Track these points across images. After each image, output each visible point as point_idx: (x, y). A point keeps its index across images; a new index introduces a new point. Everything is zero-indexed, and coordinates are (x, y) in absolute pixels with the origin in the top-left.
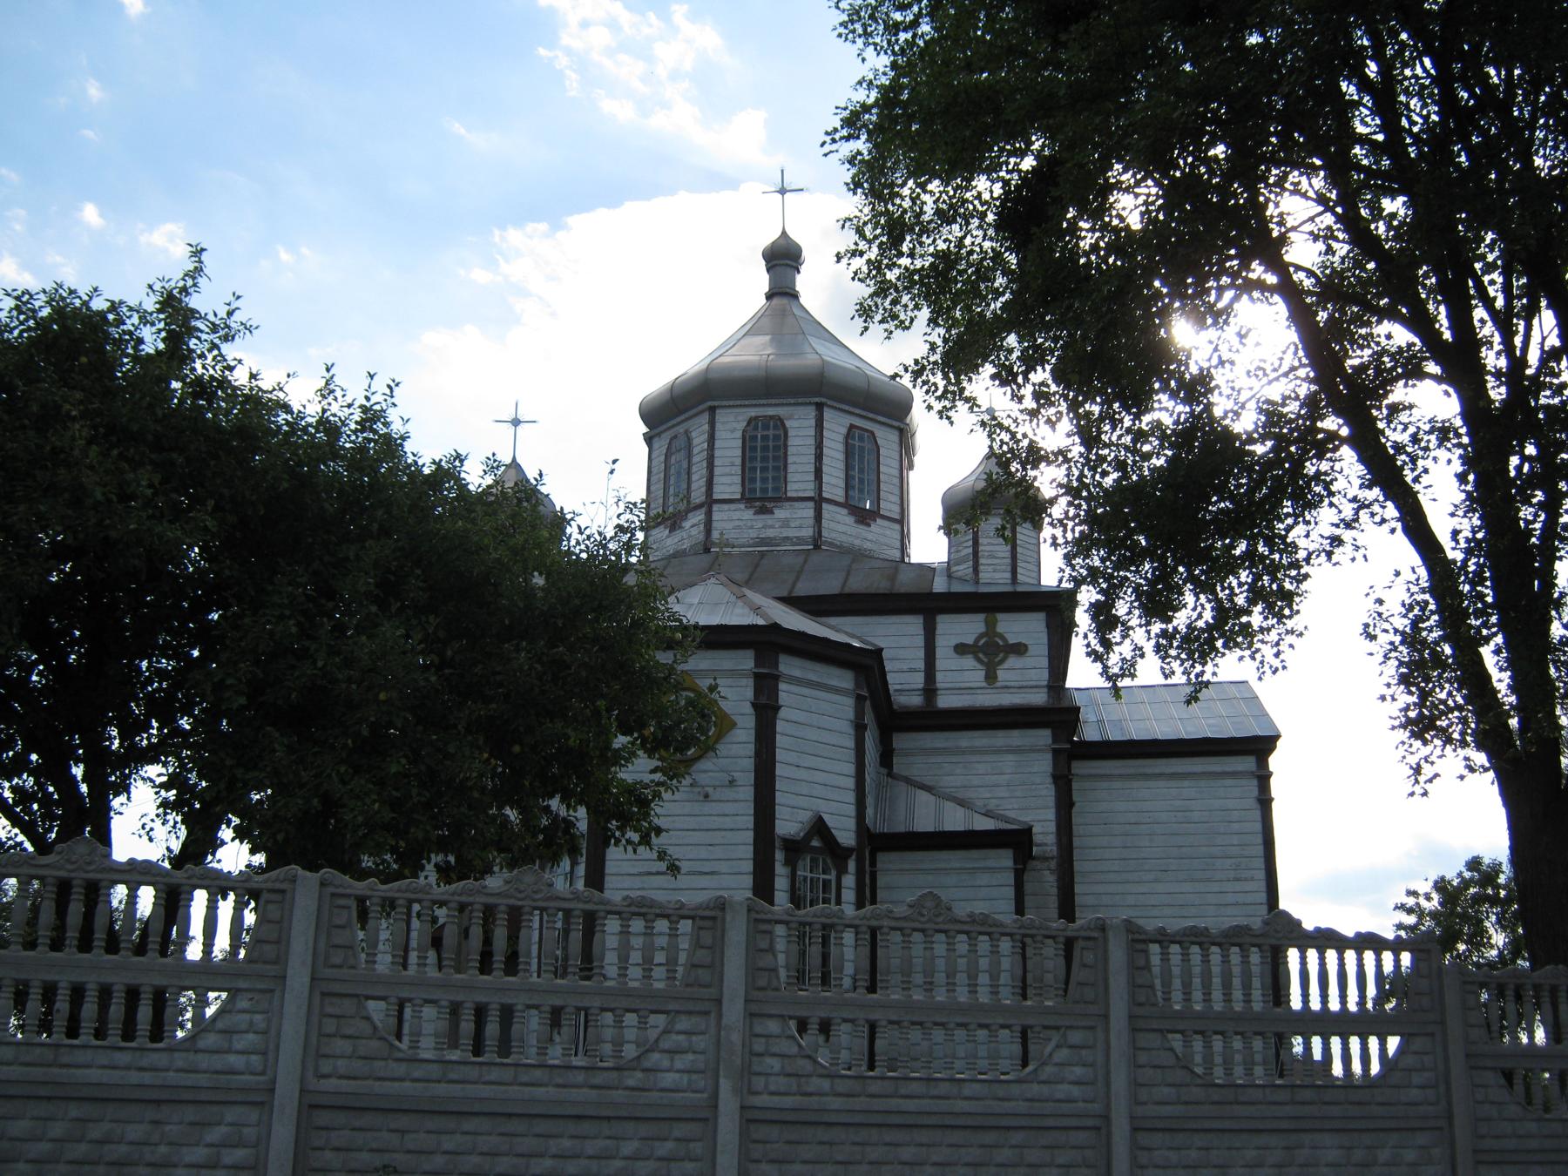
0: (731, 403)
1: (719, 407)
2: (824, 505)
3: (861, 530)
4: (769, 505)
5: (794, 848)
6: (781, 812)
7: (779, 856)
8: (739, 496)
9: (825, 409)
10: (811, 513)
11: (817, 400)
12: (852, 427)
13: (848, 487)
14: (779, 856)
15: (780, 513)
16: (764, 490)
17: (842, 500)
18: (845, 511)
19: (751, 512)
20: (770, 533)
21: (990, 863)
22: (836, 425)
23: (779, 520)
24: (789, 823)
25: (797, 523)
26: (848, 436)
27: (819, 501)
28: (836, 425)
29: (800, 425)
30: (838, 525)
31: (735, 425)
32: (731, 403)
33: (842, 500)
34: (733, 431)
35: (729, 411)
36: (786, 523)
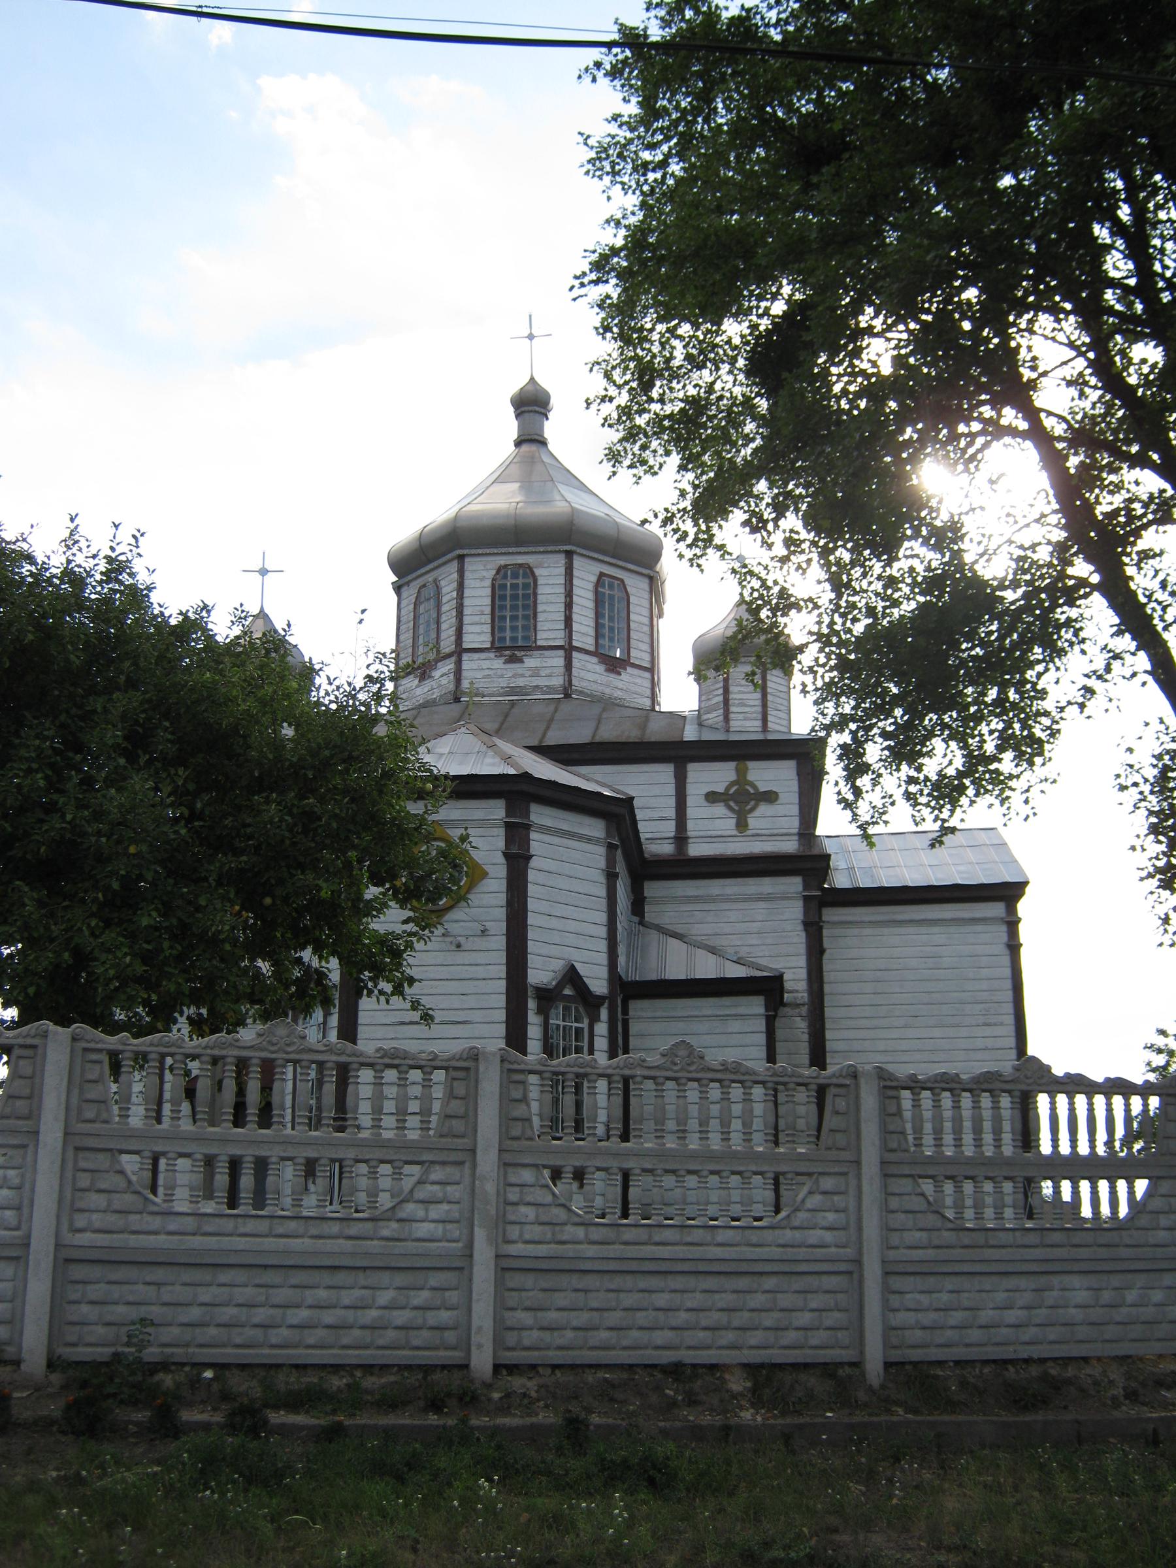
2: (575, 654)
3: (612, 678)
4: (519, 654)
8: (488, 646)
9: (575, 557)
10: (560, 662)
11: (568, 548)
12: (602, 575)
13: (598, 636)
15: (531, 662)
16: (514, 639)
18: (595, 660)
20: (520, 682)
22: (586, 573)
23: (529, 669)
26: (599, 583)
27: (569, 649)
28: (586, 573)
31: (485, 573)
33: (592, 648)
34: (483, 579)
36: (536, 673)
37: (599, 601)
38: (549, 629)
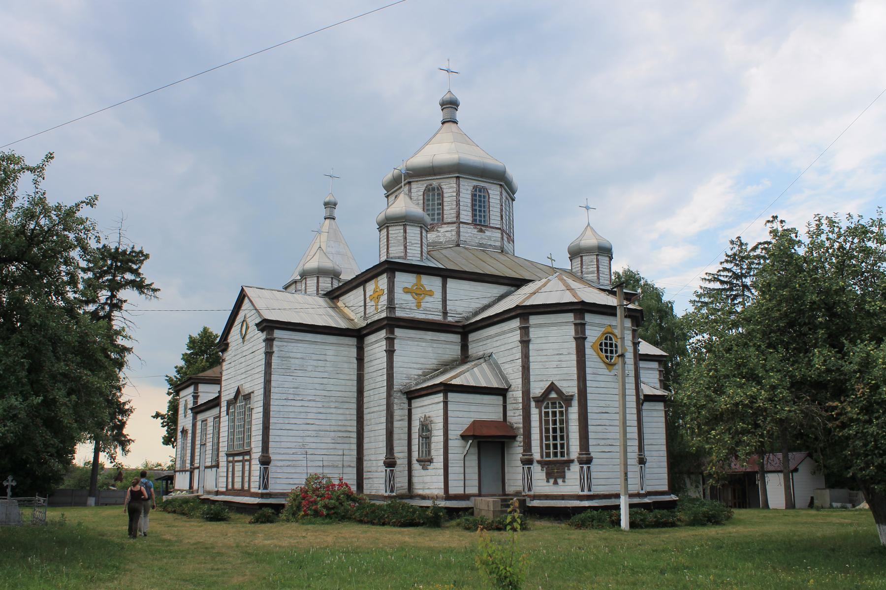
0: (467, 177)
1: (462, 177)
4: (483, 228)
5: (539, 401)
6: (533, 385)
7: (533, 404)
8: (471, 222)
12: (475, 188)
13: (474, 215)
14: (533, 404)
15: (488, 233)
16: (480, 221)
19: (476, 230)
20: (484, 242)
21: (657, 408)
22: (467, 187)
23: (487, 236)
24: (537, 389)
25: (495, 238)
27: (458, 222)
29: (449, 187)
30: (469, 233)
31: (468, 187)
32: (467, 177)
34: (467, 190)
35: (465, 180)
36: (489, 238)
37: (473, 200)
38: (449, 213)
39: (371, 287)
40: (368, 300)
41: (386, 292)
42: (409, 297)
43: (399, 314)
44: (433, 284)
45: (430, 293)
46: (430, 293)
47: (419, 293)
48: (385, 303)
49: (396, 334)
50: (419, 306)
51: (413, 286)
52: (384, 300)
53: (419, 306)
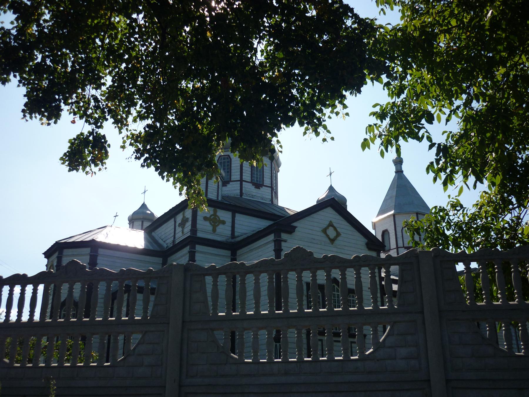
2: (244, 183)
17: (250, 181)
18: (251, 184)
30: (248, 188)
33: (250, 181)
38: (236, 175)
39: (179, 218)
40: (177, 227)
41: (190, 219)
42: (207, 223)
43: (200, 235)
44: (225, 215)
45: (223, 222)
46: (223, 222)
47: (215, 221)
48: (190, 228)
49: (196, 249)
50: (214, 230)
51: (211, 216)
52: (188, 226)
53: (214, 230)
